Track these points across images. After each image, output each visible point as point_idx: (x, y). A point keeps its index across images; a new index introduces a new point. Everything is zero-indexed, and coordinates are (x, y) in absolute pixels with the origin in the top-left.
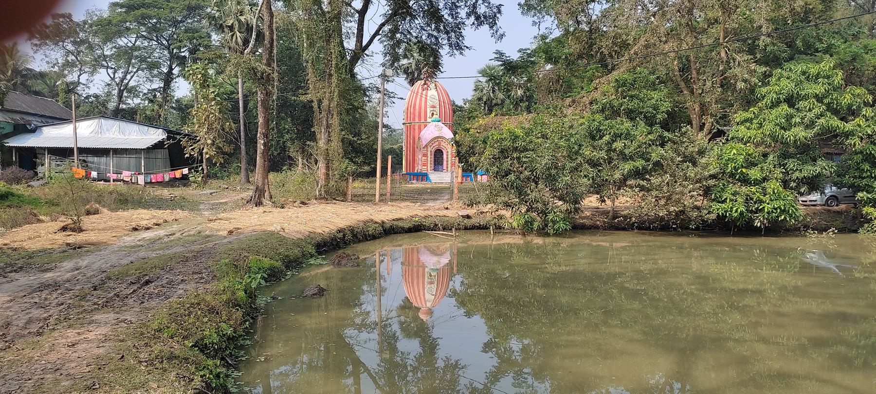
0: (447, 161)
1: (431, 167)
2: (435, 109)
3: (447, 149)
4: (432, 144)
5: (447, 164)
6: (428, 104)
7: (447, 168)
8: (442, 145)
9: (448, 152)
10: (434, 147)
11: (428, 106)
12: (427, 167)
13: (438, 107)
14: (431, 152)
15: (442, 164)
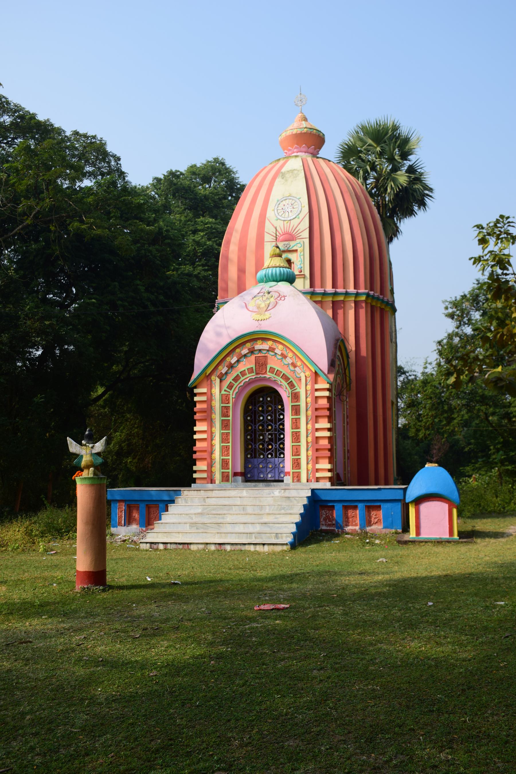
0: (296, 437)
1: (225, 464)
2: (292, 243)
3: (291, 385)
4: (231, 366)
5: (296, 452)
6: (269, 228)
7: (297, 464)
8: (272, 370)
9: (296, 397)
10: (236, 379)
11: (267, 238)
12: (210, 465)
13: (306, 234)
14: (225, 399)
15: (281, 451)
